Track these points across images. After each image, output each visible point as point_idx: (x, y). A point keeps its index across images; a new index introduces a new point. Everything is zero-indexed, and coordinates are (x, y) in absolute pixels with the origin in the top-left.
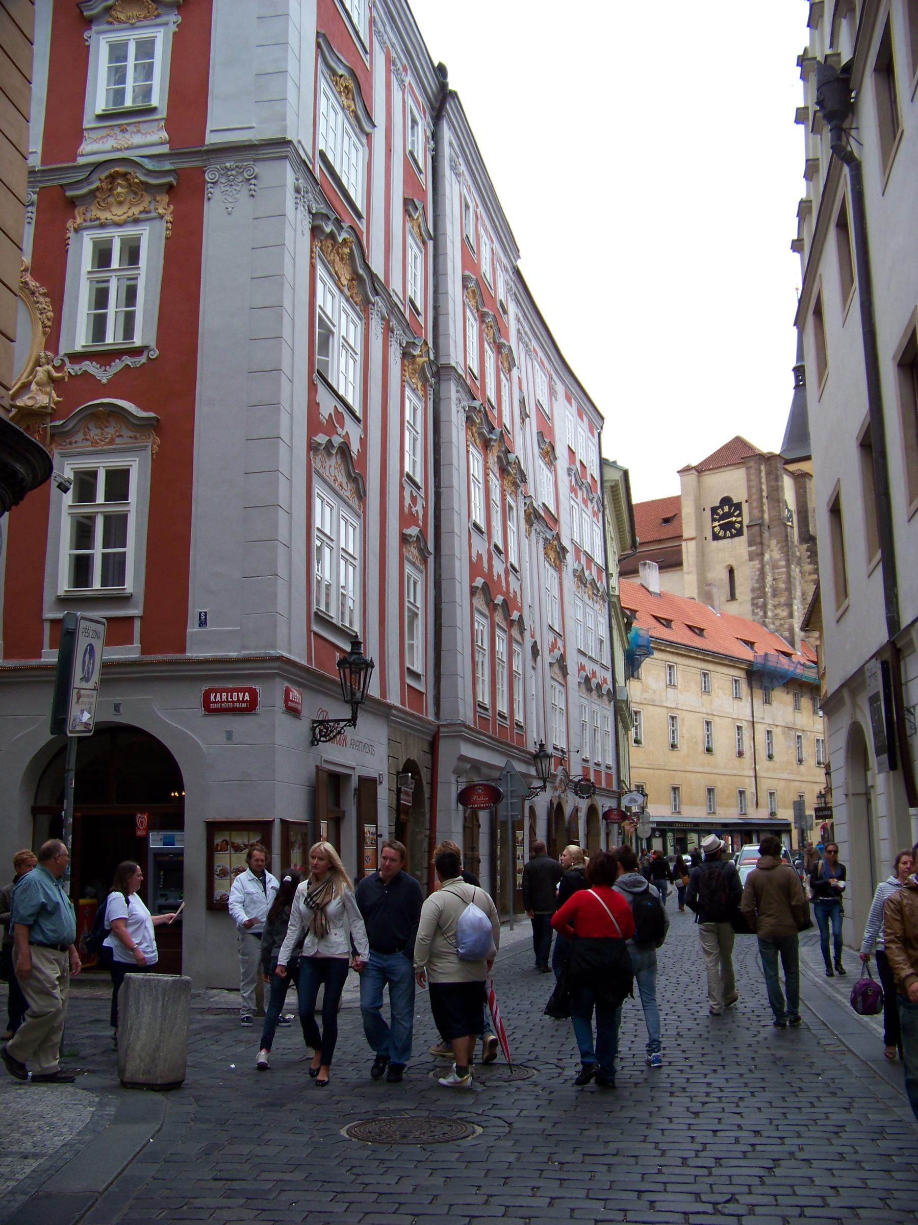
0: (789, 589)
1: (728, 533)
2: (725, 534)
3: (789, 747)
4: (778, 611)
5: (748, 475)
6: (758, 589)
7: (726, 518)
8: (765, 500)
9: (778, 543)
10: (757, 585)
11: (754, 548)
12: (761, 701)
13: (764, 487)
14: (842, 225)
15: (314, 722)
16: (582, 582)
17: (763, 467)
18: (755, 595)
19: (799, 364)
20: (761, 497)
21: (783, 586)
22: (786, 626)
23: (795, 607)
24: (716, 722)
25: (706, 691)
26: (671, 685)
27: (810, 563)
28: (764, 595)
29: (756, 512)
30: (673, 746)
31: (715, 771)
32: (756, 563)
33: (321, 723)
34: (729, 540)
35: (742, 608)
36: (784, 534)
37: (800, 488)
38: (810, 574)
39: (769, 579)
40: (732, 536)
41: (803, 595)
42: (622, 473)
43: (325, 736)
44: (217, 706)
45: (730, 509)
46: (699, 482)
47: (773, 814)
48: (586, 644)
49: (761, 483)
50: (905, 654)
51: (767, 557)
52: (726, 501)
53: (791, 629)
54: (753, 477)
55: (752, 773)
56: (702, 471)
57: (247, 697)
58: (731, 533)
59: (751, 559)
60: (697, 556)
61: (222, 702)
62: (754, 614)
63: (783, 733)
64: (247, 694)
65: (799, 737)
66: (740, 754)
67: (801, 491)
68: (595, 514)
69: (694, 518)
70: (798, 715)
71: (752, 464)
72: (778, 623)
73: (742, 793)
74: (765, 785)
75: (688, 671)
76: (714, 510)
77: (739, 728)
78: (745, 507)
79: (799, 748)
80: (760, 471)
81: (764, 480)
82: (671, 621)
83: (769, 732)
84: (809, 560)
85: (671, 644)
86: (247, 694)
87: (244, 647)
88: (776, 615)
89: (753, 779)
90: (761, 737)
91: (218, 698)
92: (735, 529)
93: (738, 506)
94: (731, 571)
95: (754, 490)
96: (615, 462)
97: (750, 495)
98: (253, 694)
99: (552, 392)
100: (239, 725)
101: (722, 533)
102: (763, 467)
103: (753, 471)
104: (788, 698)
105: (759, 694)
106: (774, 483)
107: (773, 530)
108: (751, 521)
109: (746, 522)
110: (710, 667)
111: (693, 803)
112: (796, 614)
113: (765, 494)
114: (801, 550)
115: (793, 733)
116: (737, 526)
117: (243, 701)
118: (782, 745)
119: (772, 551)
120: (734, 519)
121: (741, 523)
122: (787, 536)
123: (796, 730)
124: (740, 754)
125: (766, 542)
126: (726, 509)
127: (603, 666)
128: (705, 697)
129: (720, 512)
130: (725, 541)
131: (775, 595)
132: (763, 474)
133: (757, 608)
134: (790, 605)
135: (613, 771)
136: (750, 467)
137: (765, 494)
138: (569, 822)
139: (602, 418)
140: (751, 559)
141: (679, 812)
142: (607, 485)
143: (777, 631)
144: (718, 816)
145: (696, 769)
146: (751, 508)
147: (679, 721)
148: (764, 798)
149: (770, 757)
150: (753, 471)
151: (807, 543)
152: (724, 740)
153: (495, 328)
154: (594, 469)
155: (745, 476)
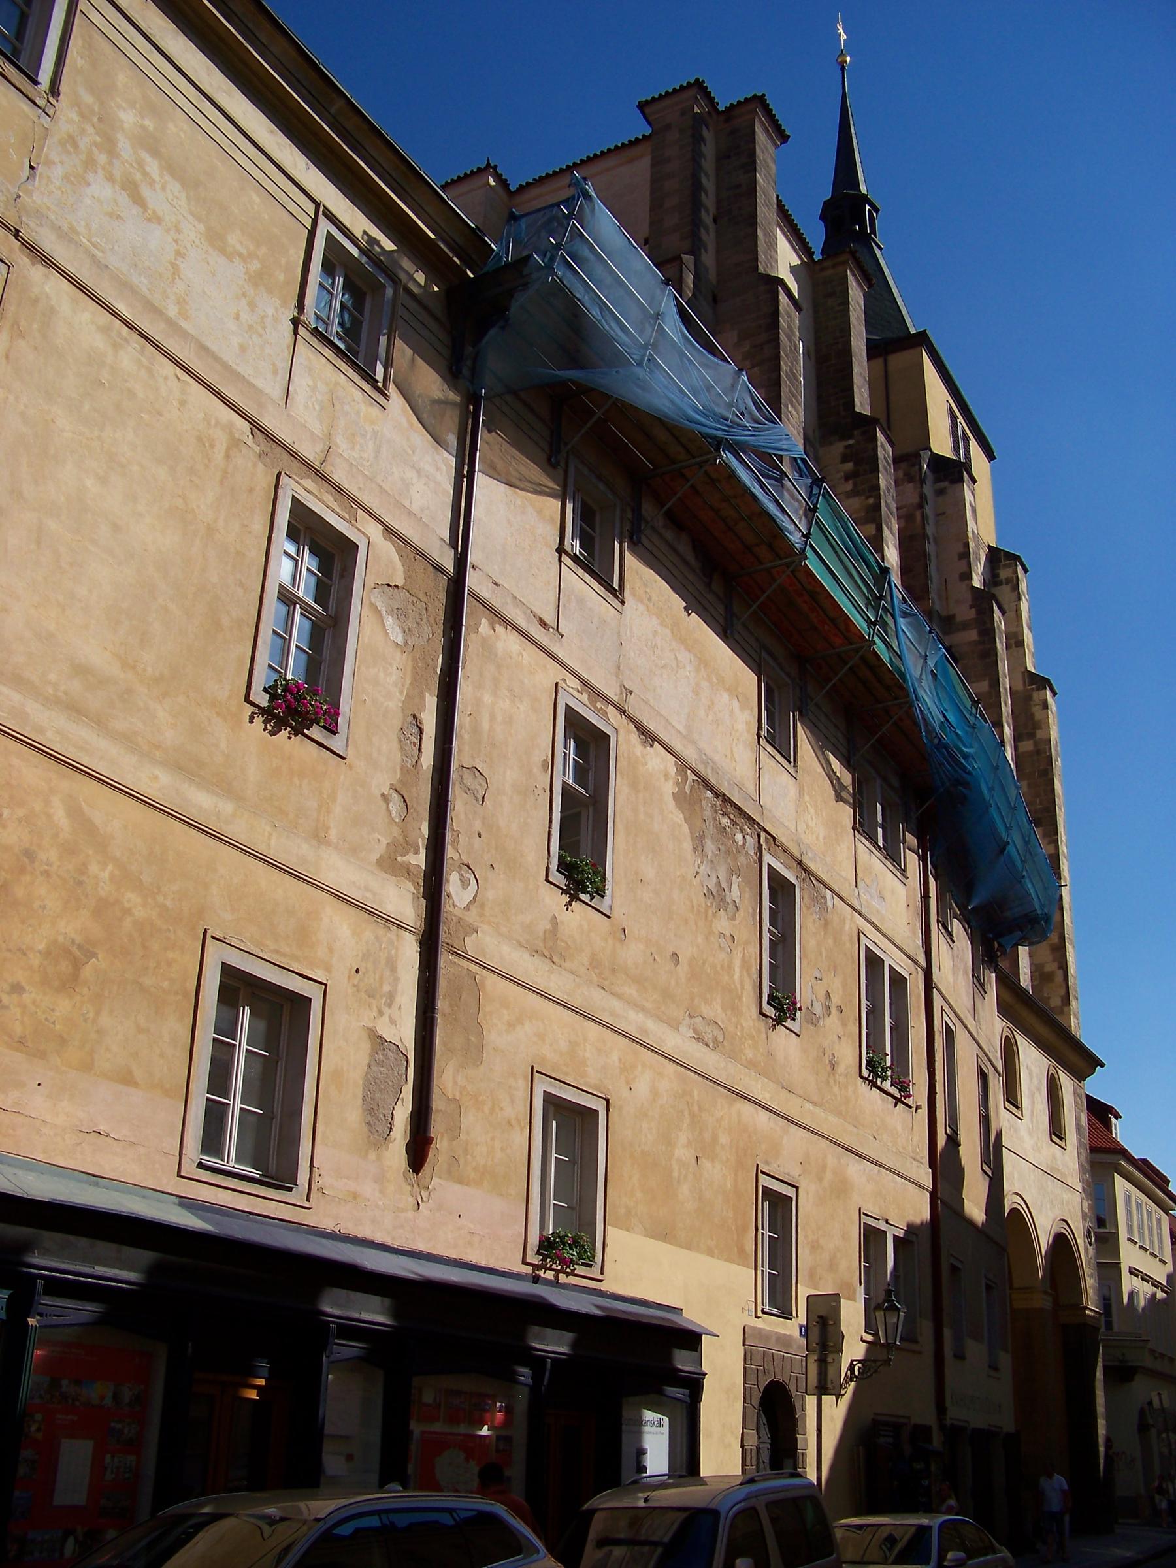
3: (718, 897)
8: (707, 219)
13: (709, 183)
20: (696, 204)
27: (854, 493)
83: (588, 743)
84: (849, 486)
89: (410, 952)
113: (709, 200)
123: (766, 839)
132: (709, 150)
151: (843, 438)
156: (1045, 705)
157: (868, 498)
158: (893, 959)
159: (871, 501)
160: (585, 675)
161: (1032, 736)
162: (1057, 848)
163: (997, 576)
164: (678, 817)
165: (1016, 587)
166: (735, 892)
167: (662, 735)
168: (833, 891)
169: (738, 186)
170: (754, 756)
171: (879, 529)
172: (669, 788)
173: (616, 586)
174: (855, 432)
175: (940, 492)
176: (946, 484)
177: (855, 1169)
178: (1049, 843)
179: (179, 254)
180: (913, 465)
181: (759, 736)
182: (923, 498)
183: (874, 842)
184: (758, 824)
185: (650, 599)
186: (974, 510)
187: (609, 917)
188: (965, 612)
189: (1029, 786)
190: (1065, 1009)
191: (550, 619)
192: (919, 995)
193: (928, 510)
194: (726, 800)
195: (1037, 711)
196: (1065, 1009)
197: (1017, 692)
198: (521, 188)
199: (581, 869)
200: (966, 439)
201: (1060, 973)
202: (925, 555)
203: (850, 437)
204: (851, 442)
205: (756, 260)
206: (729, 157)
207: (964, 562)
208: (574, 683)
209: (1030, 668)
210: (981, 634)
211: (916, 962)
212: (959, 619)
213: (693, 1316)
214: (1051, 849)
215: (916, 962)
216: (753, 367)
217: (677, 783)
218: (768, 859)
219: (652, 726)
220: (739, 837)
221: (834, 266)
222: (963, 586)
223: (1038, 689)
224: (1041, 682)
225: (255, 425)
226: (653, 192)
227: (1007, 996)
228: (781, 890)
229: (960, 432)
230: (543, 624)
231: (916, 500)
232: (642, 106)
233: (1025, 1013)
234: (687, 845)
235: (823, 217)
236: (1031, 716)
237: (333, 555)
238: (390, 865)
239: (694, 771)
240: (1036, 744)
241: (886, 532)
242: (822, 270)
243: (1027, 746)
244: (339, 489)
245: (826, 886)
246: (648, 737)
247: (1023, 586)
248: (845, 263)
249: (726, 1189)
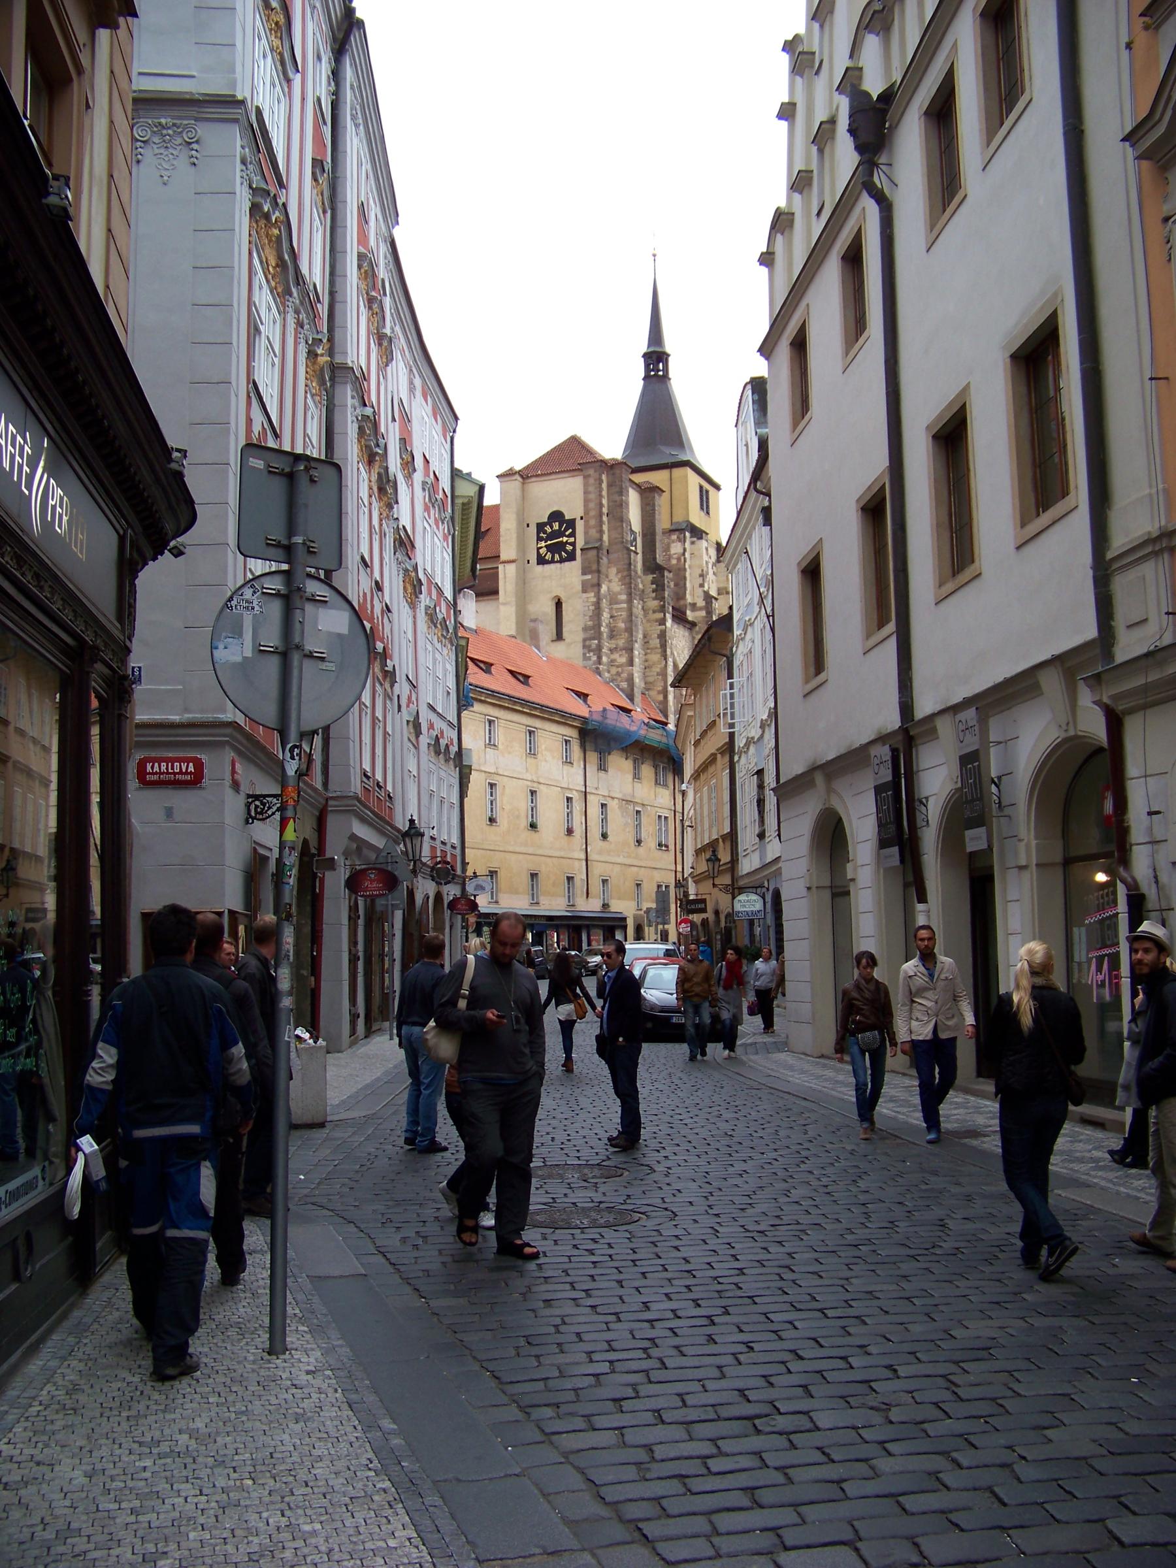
0: (630, 631)
1: (557, 557)
2: (553, 557)
3: (626, 824)
4: (615, 656)
5: (586, 485)
6: (593, 628)
7: (555, 537)
8: (605, 518)
10: (590, 623)
11: (589, 577)
12: (595, 768)
13: (605, 502)
14: (853, 259)
15: (249, 796)
16: (432, 621)
17: (604, 477)
18: (588, 635)
19: (651, 349)
21: (622, 625)
22: (625, 675)
23: (636, 653)
24: (543, 791)
25: (532, 752)
26: (491, 744)
28: (598, 636)
29: (593, 533)
30: (492, 820)
31: (540, 852)
32: (591, 597)
33: (257, 797)
34: (558, 565)
35: (570, 650)
36: (627, 562)
37: (648, 504)
38: (654, 612)
39: (606, 615)
40: (562, 561)
41: (645, 637)
42: (477, 488)
43: (261, 813)
44: (156, 777)
45: (560, 527)
46: (523, 490)
47: (605, 906)
48: (434, 697)
49: (601, 496)
50: (918, 742)
51: (604, 588)
52: (557, 516)
53: (630, 680)
54: (591, 489)
55: (584, 857)
56: (528, 477)
57: (191, 768)
58: (560, 556)
59: (584, 591)
60: (517, 584)
61: (161, 773)
62: (585, 658)
63: (620, 807)
64: (191, 765)
65: (638, 812)
66: (570, 832)
67: (648, 508)
68: (445, 538)
69: (514, 536)
70: (638, 786)
71: (591, 472)
72: (614, 670)
73: (570, 879)
74: (597, 871)
75: (511, 727)
76: (540, 527)
77: (569, 799)
78: (580, 526)
79: (638, 826)
80: (601, 482)
81: (604, 493)
82: (492, 665)
83: (603, 805)
85: (493, 693)
86: (191, 765)
87: (187, 710)
88: (613, 661)
90: (594, 811)
91: (156, 769)
92: (566, 551)
93: (572, 523)
94: (559, 604)
95: (592, 505)
96: (469, 474)
97: (587, 511)
98: (199, 765)
99: (412, 388)
100: (180, 800)
101: (549, 556)
102: (604, 477)
103: (591, 481)
104: (628, 765)
105: (593, 757)
106: (617, 498)
107: (613, 556)
108: (586, 543)
109: (580, 543)
110: (537, 723)
111: (514, 891)
112: (637, 660)
113: (605, 510)
114: (644, 582)
115: (631, 807)
116: (569, 548)
117: (186, 773)
118: (618, 822)
119: (610, 581)
120: (565, 539)
121: (573, 544)
122: (630, 564)
123: (635, 803)
124: (570, 832)
125: (603, 569)
126: (556, 526)
127: (450, 724)
128: (531, 760)
130: (552, 566)
131: (612, 636)
132: (604, 486)
133: (590, 651)
134: (630, 650)
135: (458, 852)
136: (589, 476)
137: (605, 510)
138: (420, 913)
139: (456, 418)
140: (584, 591)
141: (497, 902)
142: (459, 501)
143: (613, 681)
144: (542, 907)
145: (518, 849)
146: (587, 527)
147: (499, 789)
148: (595, 886)
149: (604, 836)
150: (591, 481)
152: (551, 814)
153: (380, 315)
154: (445, 483)
155: (582, 487)
158: (665, 813)
175: (693, 543)
177: (655, 873)
182: (685, 550)
188: (701, 603)
193: (687, 555)
200: (707, 492)
202: (685, 578)
213: (626, 914)
249: (630, 885)
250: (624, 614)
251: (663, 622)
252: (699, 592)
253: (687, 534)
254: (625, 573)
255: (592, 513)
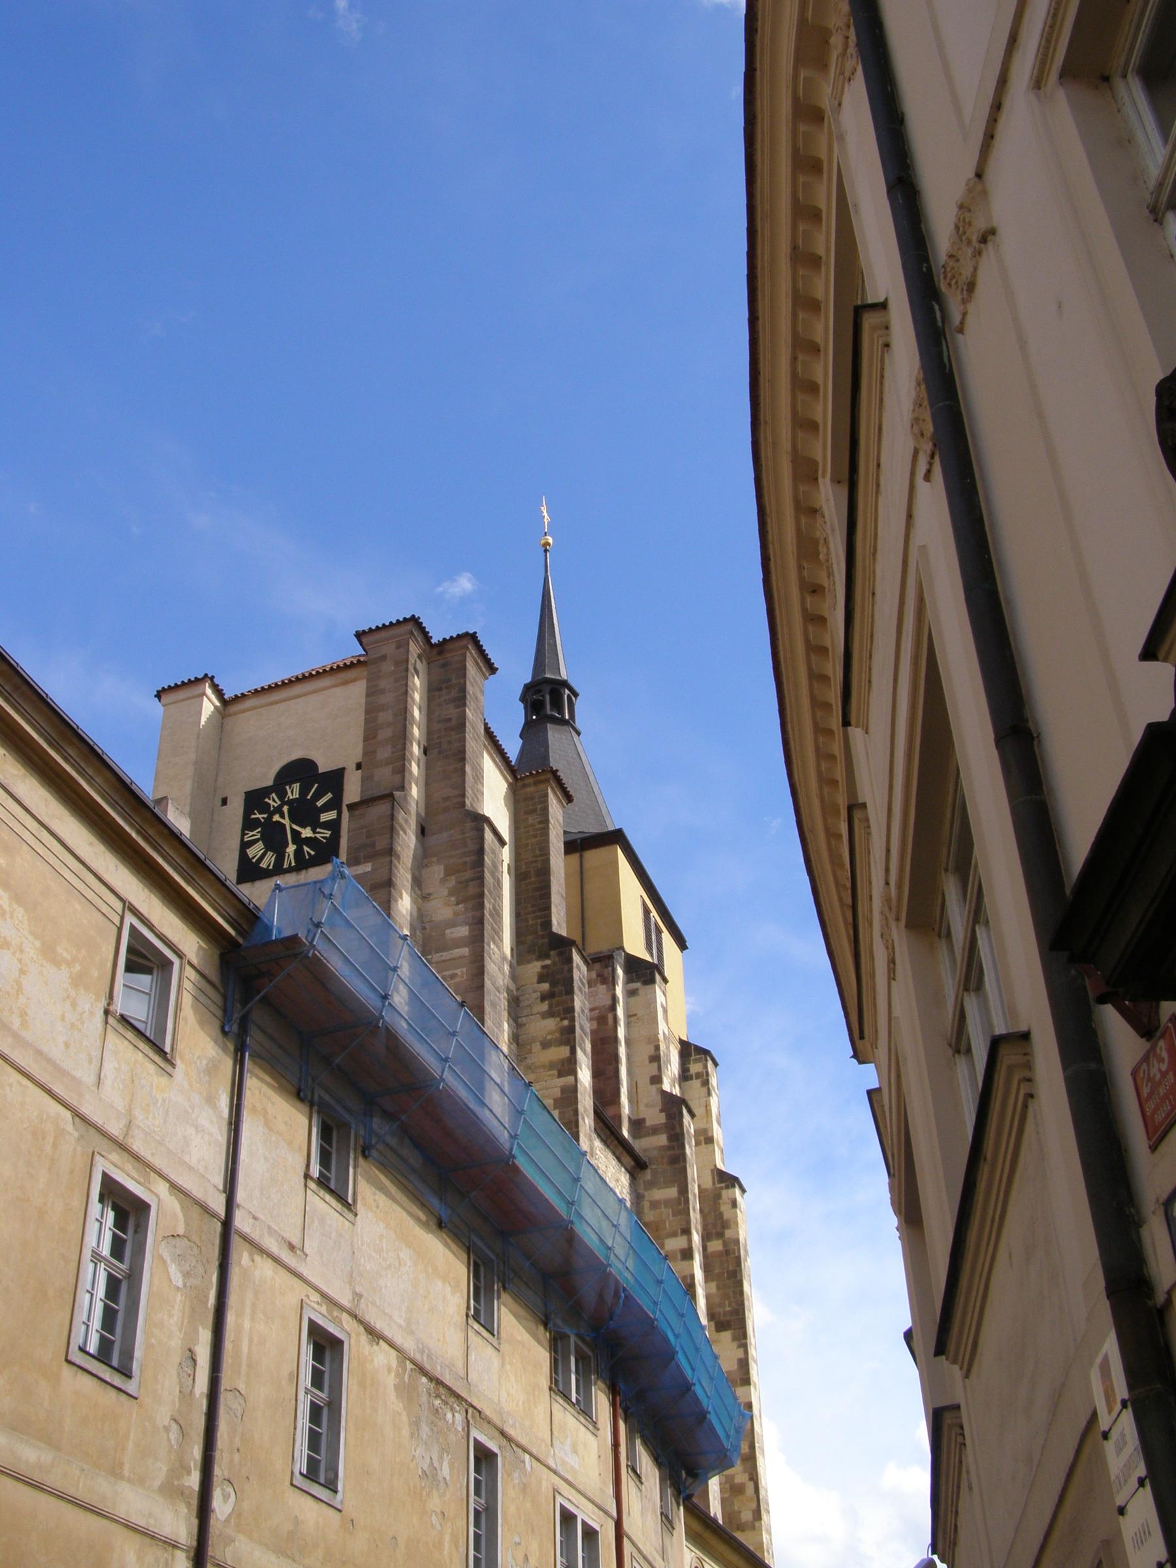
9: (449, 872)
36: (472, 846)
38: (545, 1045)
40: (302, 863)
45: (304, 791)
54: (383, 684)
63: (406, 1391)
67: (531, 819)
83: (325, 1346)
84: (545, 1006)
93: (335, 780)
103: (388, 667)
106: (451, 711)
121: (334, 826)
123: (473, 1412)
126: (293, 792)
129: (273, 801)
136: (383, 658)
151: (542, 956)
156: (734, 1204)
157: (562, 1019)
158: (586, 1514)
159: (566, 1023)
160: (324, 1288)
161: (720, 1235)
162: (746, 1352)
163: (688, 1070)
164: (399, 1406)
165: (706, 1083)
166: (445, 1471)
167: (388, 1333)
168: (531, 1454)
169: (450, 720)
170: (461, 1335)
171: (573, 1052)
172: (391, 1380)
173: (350, 1201)
174: (552, 953)
175: (631, 993)
176: (638, 985)
178: (739, 1347)
179: (22, 972)
180: (607, 967)
181: (467, 1316)
182: (614, 999)
183: (567, 1398)
184: (466, 1401)
185: (377, 1207)
186: (665, 1011)
187: (340, 1511)
188: (655, 1116)
189: (718, 1288)
190: (757, 1524)
191: (296, 1241)
192: (609, 1544)
194: (439, 1382)
195: (725, 1208)
196: (757, 1524)
197: (706, 1190)
198: (236, 698)
199: (320, 1471)
200: (659, 932)
201: (751, 1485)
203: (547, 956)
204: (548, 962)
205: (464, 795)
206: (440, 689)
207: (655, 1065)
208: (315, 1297)
209: (720, 1165)
210: (670, 1138)
211: (606, 1512)
212: (648, 1123)
214: (740, 1353)
215: (606, 1512)
216: (458, 904)
217: (397, 1375)
218: (475, 1433)
219: (380, 1325)
220: (449, 1416)
221: (536, 784)
222: (654, 1088)
223: (727, 1187)
224: (731, 1181)
225: (77, 1114)
226: (367, 721)
227: (697, 1526)
228: (484, 1458)
229: (653, 927)
230: (292, 1247)
231: (609, 1002)
232: (359, 635)
233: (714, 1541)
234: (406, 1431)
235: (523, 699)
236: (720, 1215)
237: (129, 1212)
238: (171, 1491)
239: (413, 1362)
240: (725, 1244)
241: (579, 1053)
242: (524, 786)
243: (716, 1246)
244: (136, 1157)
245: (525, 1450)
246: (375, 1335)
247: (713, 1081)
248: (547, 781)
250: (462, 973)
251: (569, 1067)
252: (649, 1094)
253: (620, 972)
254: (469, 874)
255: (385, 734)
